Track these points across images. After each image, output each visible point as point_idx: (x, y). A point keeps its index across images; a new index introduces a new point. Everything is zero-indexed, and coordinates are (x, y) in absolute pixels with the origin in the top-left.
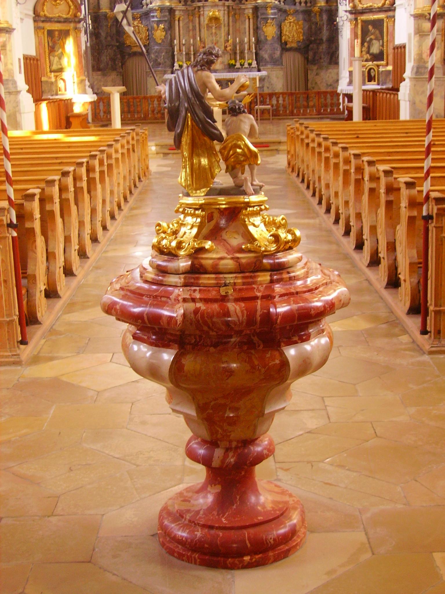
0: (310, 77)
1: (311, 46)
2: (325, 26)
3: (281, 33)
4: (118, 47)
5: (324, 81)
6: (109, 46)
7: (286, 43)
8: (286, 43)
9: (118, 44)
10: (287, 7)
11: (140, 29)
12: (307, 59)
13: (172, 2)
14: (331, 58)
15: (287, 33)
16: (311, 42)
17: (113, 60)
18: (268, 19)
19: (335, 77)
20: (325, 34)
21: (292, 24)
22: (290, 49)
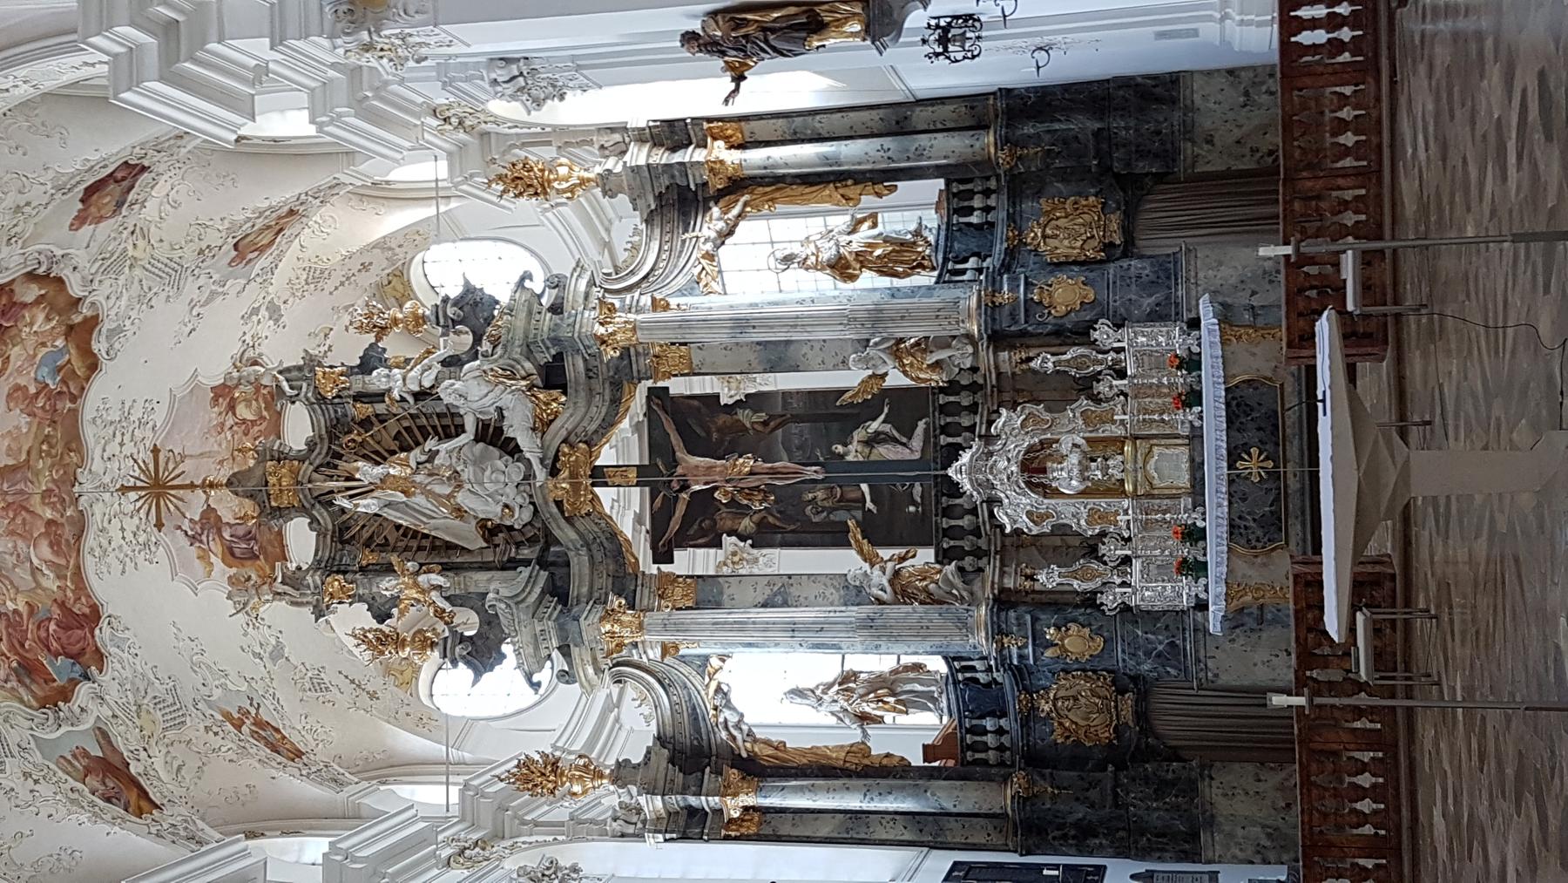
0: (1217, 166)
1: (1117, 167)
2: (1056, 126)
3: (1075, 263)
4: (1120, 767)
5: (1231, 115)
6: (1116, 795)
7: (1108, 247)
8: (1108, 247)
9: (1110, 768)
10: (999, 248)
11: (1061, 694)
12: (1160, 178)
13: (979, 594)
14: (1159, 100)
15: (1079, 244)
16: (1106, 169)
17: (1162, 787)
18: (1028, 302)
19: (1221, 81)
20: (1082, 125)
21: (1049, 232)
22: (1128, 232)
